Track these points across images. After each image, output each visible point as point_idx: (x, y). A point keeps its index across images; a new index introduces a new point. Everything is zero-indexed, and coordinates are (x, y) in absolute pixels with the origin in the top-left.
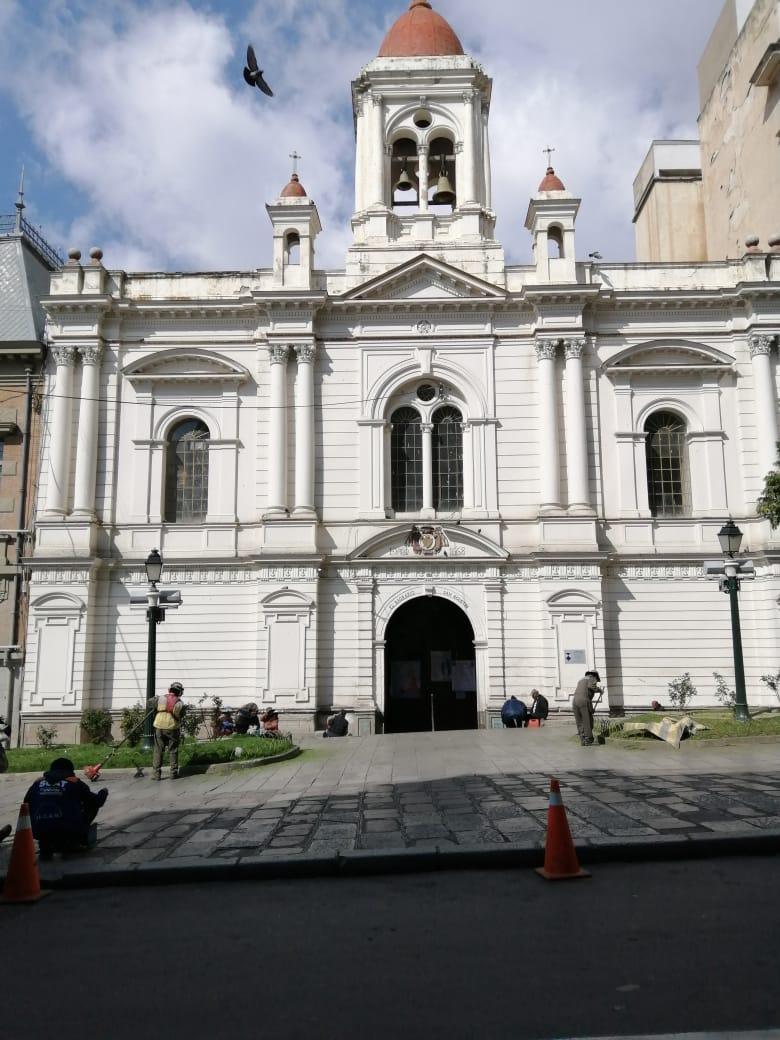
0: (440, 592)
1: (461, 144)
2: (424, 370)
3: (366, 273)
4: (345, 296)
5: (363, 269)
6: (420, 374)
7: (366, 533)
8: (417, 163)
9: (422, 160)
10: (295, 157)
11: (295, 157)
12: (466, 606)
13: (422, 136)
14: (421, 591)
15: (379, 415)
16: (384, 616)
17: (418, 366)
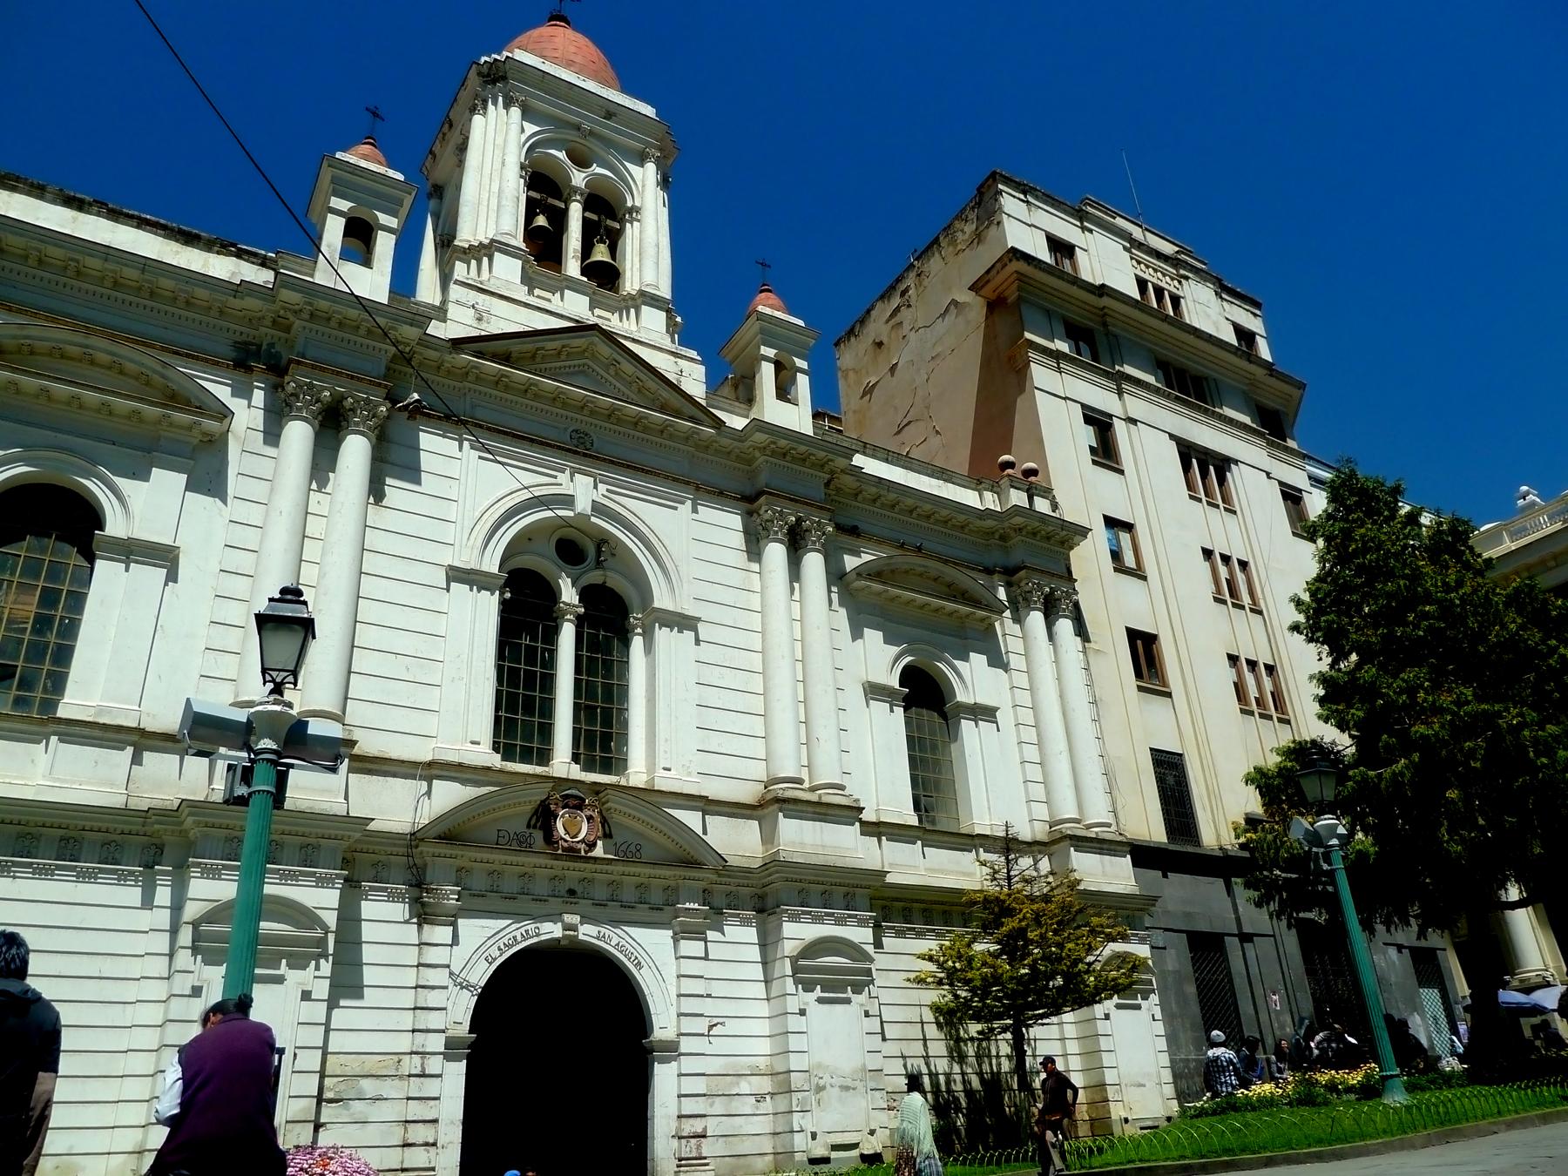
0: (587, 933)
1: (635, 210)
2: (583, 505)
3: (484, 325)
4: (458, 344)
5: (480, 319)
6: (571, 514)
7: (449, 795)
8: (566, 210)
9: (576, 212)
10: (375, 115)
11: (375, 115)
12: (639, 965)
13: (579, 178)
14: (552, 931)
15: (491, 564)
16: (473, 979)
17: (567, 501)
